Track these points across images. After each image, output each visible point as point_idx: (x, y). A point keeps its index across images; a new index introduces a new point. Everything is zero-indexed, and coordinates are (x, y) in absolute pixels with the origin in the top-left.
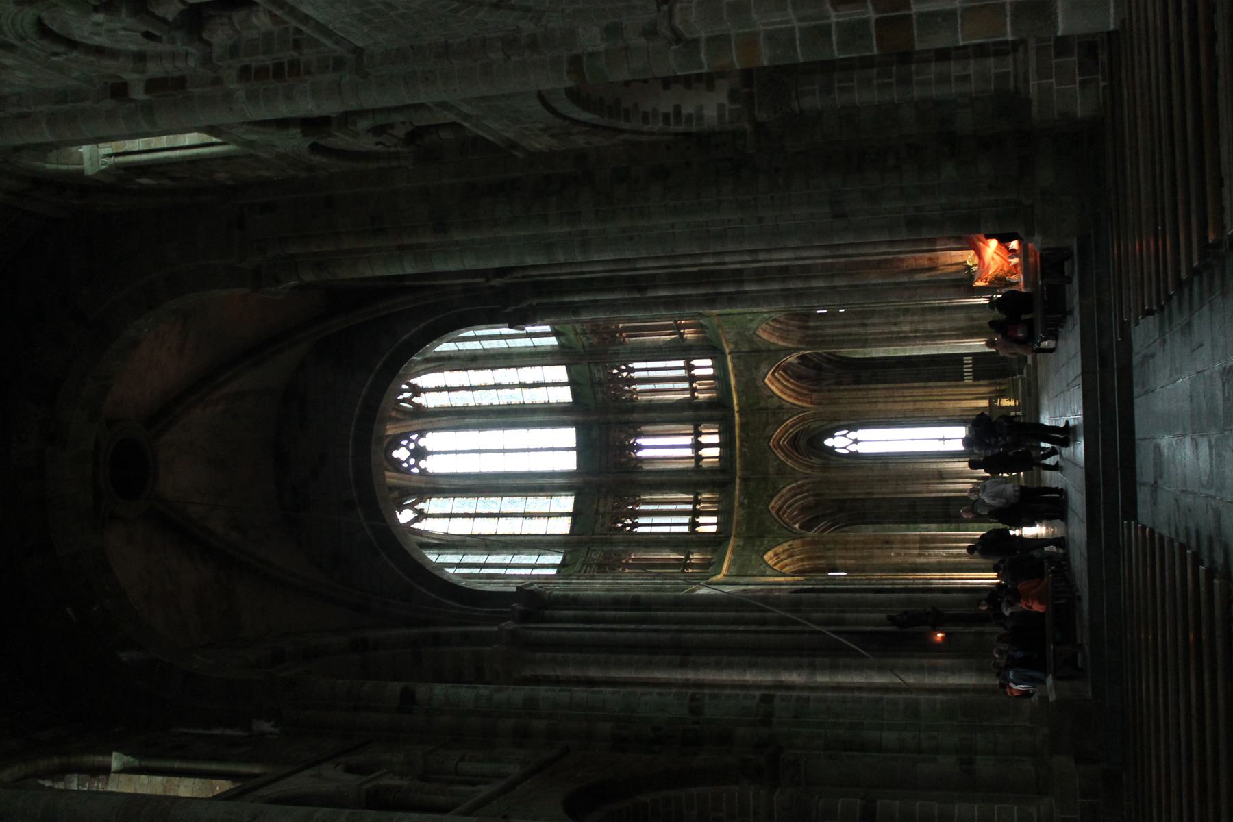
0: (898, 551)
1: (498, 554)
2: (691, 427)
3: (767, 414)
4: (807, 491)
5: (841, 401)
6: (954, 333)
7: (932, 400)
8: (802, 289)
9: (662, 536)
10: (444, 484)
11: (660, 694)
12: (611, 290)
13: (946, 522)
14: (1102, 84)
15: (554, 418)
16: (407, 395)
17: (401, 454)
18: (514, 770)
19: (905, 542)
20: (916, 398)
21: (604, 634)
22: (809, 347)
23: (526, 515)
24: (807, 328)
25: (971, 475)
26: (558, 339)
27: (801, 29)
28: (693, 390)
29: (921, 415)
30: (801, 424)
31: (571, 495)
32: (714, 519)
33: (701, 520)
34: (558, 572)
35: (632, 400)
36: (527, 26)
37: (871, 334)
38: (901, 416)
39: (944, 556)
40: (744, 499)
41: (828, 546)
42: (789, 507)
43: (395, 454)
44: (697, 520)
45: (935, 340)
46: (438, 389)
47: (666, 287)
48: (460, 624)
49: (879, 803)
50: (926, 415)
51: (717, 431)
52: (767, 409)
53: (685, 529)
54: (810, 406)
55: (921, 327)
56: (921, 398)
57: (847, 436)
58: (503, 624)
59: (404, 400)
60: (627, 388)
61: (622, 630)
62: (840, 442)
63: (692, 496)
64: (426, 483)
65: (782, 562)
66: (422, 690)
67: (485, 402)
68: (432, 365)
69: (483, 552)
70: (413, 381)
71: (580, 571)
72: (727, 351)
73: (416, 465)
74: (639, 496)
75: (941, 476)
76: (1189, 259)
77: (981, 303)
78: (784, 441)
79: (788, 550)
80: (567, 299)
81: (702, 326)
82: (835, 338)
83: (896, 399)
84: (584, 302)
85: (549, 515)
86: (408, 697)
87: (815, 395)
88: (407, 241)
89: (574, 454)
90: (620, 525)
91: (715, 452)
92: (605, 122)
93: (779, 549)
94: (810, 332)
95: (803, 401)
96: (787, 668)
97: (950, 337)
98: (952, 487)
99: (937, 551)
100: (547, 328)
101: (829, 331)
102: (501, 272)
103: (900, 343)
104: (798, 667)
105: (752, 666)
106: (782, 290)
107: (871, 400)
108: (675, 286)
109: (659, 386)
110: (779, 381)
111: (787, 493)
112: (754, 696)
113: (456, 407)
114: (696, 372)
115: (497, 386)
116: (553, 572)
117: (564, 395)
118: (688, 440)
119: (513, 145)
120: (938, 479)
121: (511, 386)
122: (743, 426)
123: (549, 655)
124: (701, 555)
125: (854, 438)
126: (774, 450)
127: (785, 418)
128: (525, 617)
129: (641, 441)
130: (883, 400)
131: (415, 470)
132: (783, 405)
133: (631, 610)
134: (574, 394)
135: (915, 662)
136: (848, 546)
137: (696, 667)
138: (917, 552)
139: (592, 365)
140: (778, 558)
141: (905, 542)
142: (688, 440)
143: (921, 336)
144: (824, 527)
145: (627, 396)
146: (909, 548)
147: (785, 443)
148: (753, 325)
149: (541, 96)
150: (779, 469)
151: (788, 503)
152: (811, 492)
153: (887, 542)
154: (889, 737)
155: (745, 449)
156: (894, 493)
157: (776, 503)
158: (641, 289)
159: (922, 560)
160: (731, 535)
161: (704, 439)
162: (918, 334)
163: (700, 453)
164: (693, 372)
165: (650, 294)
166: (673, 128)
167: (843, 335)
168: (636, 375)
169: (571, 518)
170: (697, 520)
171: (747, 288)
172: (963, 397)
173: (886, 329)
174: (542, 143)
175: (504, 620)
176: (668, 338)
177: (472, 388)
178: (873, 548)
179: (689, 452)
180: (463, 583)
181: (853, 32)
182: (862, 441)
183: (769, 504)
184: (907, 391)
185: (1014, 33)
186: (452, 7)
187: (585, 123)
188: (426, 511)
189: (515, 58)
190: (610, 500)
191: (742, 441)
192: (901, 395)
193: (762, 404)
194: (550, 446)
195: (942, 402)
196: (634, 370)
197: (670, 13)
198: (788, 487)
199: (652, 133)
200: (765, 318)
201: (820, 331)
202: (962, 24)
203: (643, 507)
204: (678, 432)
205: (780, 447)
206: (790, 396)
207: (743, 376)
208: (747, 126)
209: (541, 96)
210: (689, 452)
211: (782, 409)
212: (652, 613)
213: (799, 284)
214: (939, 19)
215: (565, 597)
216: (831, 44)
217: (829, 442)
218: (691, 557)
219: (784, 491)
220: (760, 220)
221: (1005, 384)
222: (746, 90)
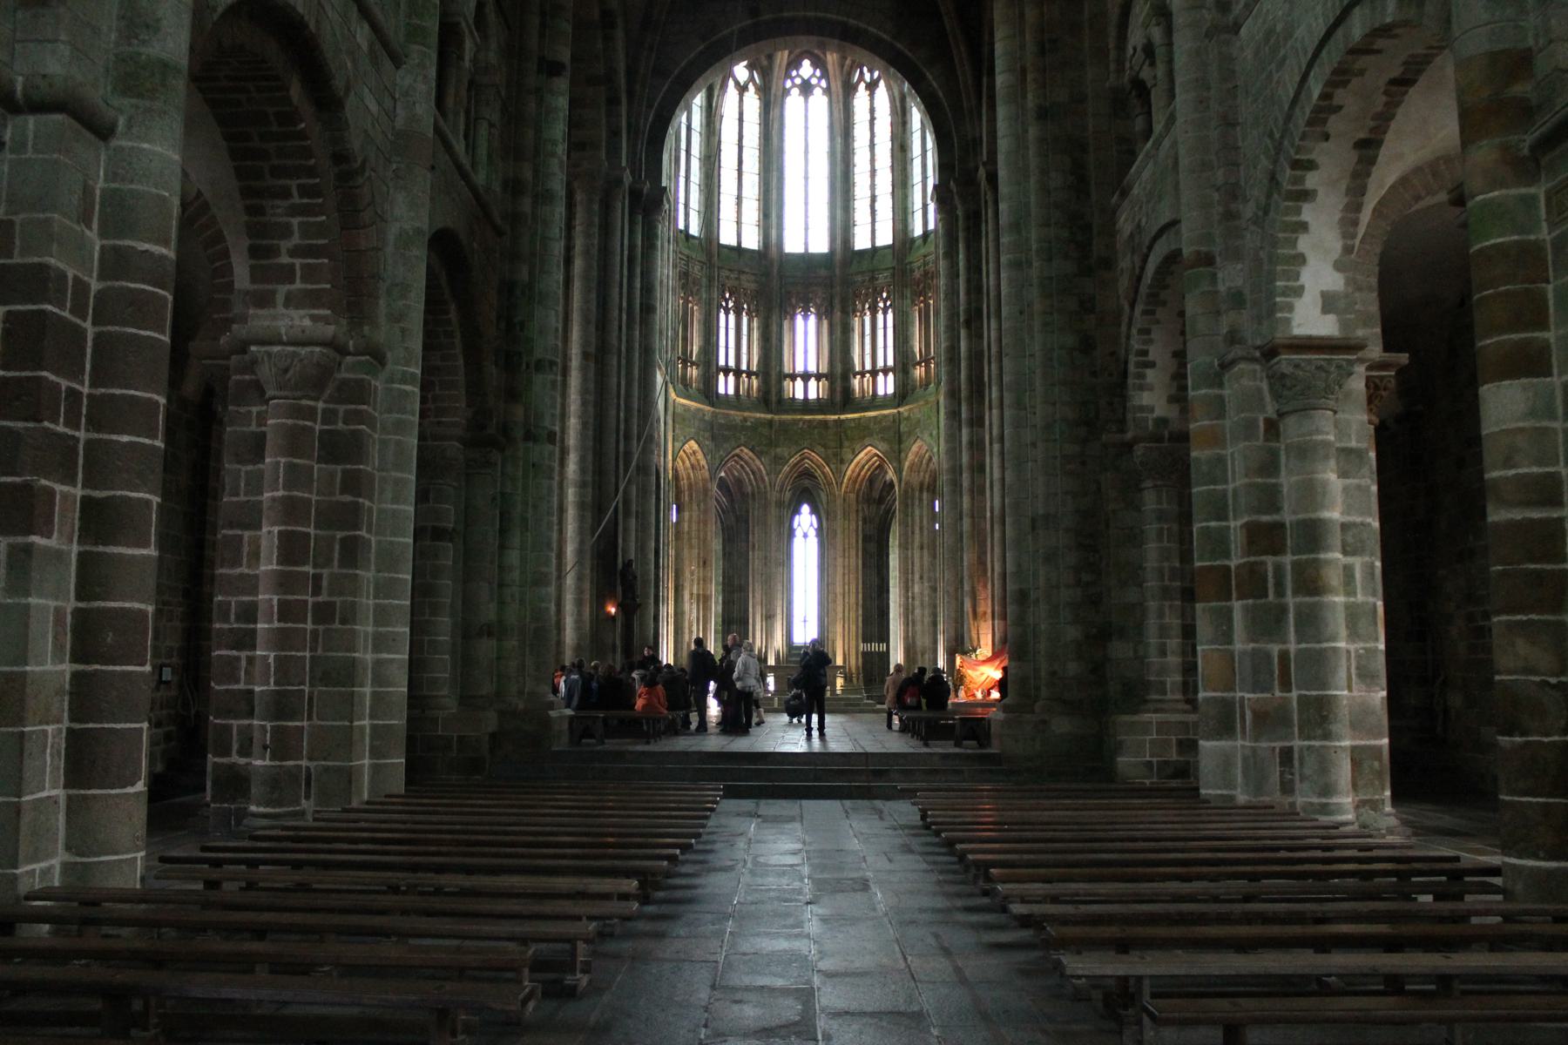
0: (696, 574)
1: (700, 168)
2: (825, 371)
4: (758, 487)
8: (961, 485)
10: (774, 113)
11: (557, 329)
12: (968, 293)
13: (723, 621)
14: (1147, 782)
15: (839, 232)
16: (867, 77)
17: (806, 69)
18: (480, 178)
19: (705, 580)
20: (847, 595)
21: (618, 277)
23: (739, 198)
24: (921, 491)
26: (919, 237)
27: (1225, 491)
28: (863, 374)
32: (731, 391)
33: (731, 378)
34: (681, 231)
35: (854, 311)
36: (1248, 210)
37: (913, 554)
42: (742, 466)
43: (806, 63)
44: (731, 374)
46: (872, 110)
47: (970, 350)
48: (629, 125)
49: (450, 545)
52: (841, 446)
53: (722, 362)
55: (917, 603)
56: (847, 600)
58: (628, 171)
59: (862, 73)
60: (867, 306)
61: (621, 294)
62: (805, 520)
64: (775, 95)
66: (562, 84)
68: (898, 104)
70: (882, 83)
71: (680, 253)
72: (901, 409)
73: (794, 85)
75: (769, 617)
76: (973, 851)
80: (961, 246)
81: (928, 384)
83: (847, 577)
84: (958, 264)
85: (739, 223)
86: (554, 69)
87: (853, 496)
88: (1029, 77)
89: (801, 250)
90: (727, 295)
91: (799, 395)
92: (1143, 290)
93: (700, 456)
94: (917, 494)
96: (582, 459)
98: (758, 627)
99: (695, 611)
100: (931, 226)
101: (917, 512)
102: (993, 178)
104: (582, 470)
105: (584, 425)
106: (961, 466)
108: (970, 358)
109: (868, 340)
112: (555, 425)
114: (881, 377)
115: (873, 172)
116: (681, 226)
117: (861, 242)
118: (812, 368)
119: (1124, 194)
121: (873, 186)
122: (825, 423)
123: (596, 220)
127: (833, 466)
128: (635, 194)
129: (812, 319)
130: (846, 564)
131: (789, 84)
133: (641, 304)
134: (862, 253)
135: (587, 585)
137: (584, 369)
138: (695, 592)
139: (891, 271)
141: (705, 580)
143: (908, 604)
145: (859, 307)
146: (698, 584)
148: (926, 436)
149: (1174, 223)
150: (780, 459)
153: (705, 563)
154: (513, 557)
155: (801, 423)
156: (753, 570)
158: (968, 323)
161: (812, 383)
163: (799, 379)
164: (881, 374)
165: (963, 333)
166: (1133, 359)
167: (913, 525)
168: (880, 316)
170: (731, 374)
171: (965, 432)
172: (846, 641)
173: (917, 568)
174: (1125, 225)
175: (632, 173)
176: (917, 350)
177: (872, 146)
178: (699, 548)
180: (671, 131)
181: (1219, 543)
185: (1207, 700)
186: (1275, 130)
187: (1142, 269)
188: (746, 94)
189: (1216, 196)
190: (753, 286)
191: (810, 421)
193: (846, 443)
194: (810, 226)
196: (885, 313)
197: (1253, 360)
199: (1128, 337)
202: (1218, 649)
203: (745, 320)
205: (803, 459)
206: (853, 471)
208: (1129, 435)
209: (1174, 223)
210: (800, 368)
212: (637, 327)
213: (966, 483)
214: (1225, 628)
215: (656, 236)
216: (1206, 520)
217: (805, 508)
220: (1034, 445)
222: (1166, 434)
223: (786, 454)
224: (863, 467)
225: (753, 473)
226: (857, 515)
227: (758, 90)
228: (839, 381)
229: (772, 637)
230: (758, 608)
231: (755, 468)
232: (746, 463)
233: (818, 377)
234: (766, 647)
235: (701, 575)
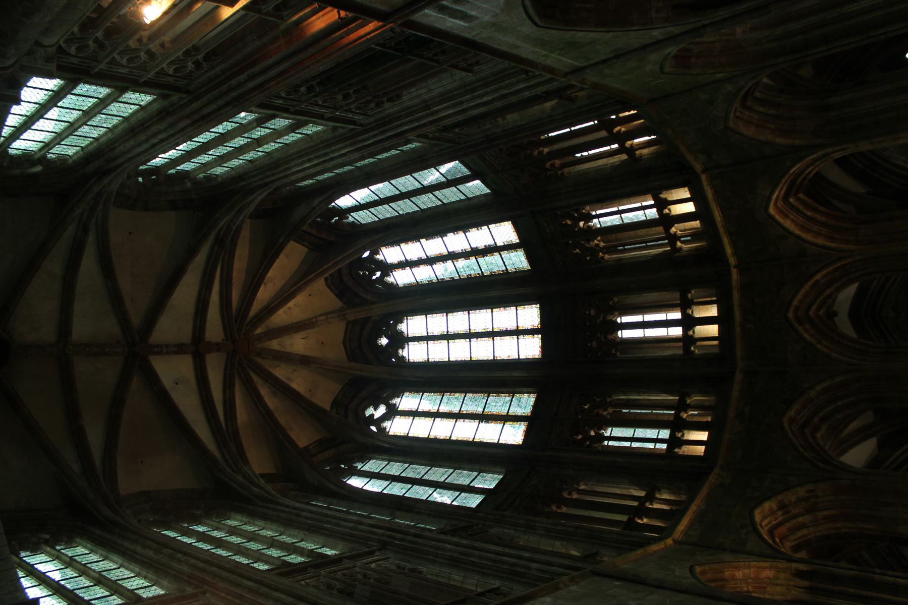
1: (440, 467)
9: (619, 459)
28: (673, 238)
31: (533, 393)
32: (703, 436)
51: (715, 299)
63: (677, 398)
65: (794, 521)
67: (447, 276)
69: (427, 462)
72: (698, 168)
74: (610, 396)
91: (713, 330)
93: (790, 497)
110: (798, 211)
113: (422, 284)
116: (473, 501)
117: (518, 261)
121: (466, 255)
124: (674, 493)
126: (796, 325)
142: (676, 315)
163: (691, 333)
164: (666, 211)
169: (526, 423)
179: (677, 331)
198: (819, 388)
204: (671, 303)
218: (658, 496)
224: (809, 219)
227: (399, 394)
233: (685, 305)
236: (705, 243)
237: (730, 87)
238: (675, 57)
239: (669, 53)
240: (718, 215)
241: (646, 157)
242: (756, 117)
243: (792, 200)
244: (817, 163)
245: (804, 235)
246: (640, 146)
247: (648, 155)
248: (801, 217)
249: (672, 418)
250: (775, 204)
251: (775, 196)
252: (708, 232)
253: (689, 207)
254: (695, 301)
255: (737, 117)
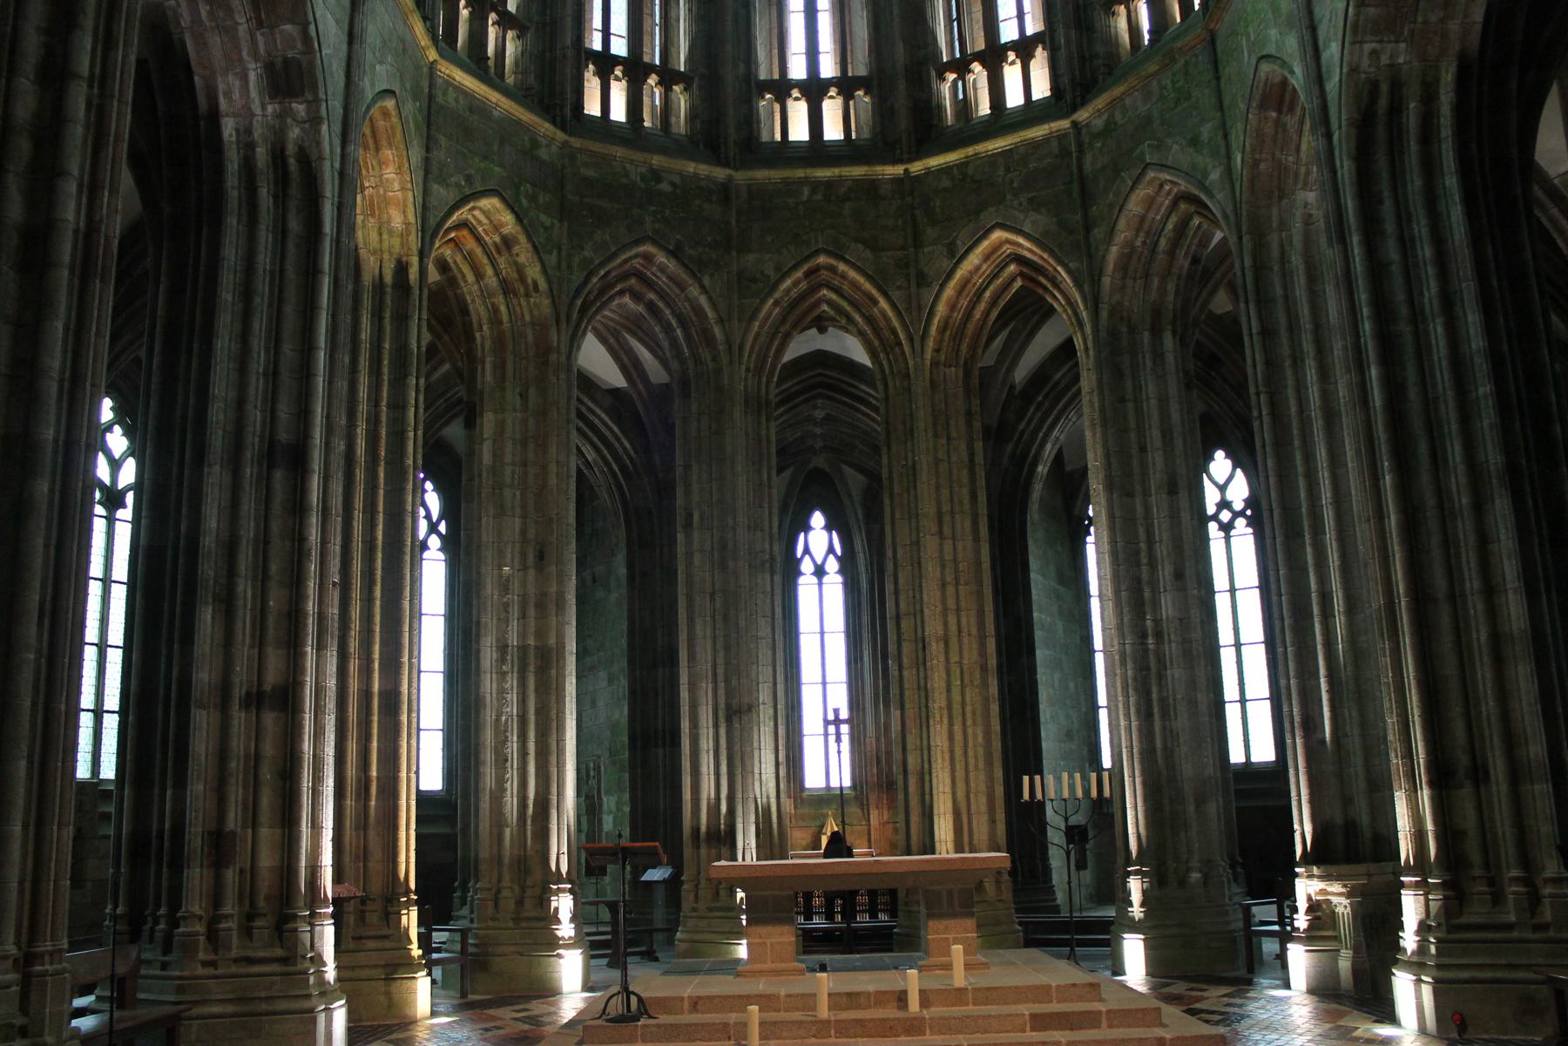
3: (902, 248)
4: (697, 360)
5: (943, 441)
6: (1159, 744)
7: (949, 690)
19: (543, 606)
22: (1103, 334)
24: (1156, 332)
25: (739, 795)
28: (961, 67)
29: (905, 661)
30: (876, 343)
32: (618, 113)
37: (1147, 509)
38: (902, 605)
39: (498, 720)
40: (673, 185)
41: (532, 391)
45: (1136, 690)
50: (906, 673)
52: (918, 244)
54: (928, 355)
55: (1172, 649)
56: (954, 658)
57: (831, 556)
62: (818, 538)
63: (682, 69)
65: (485, 261)
72: (1082, 115)
75: (736, 713)
77: (1296, 826)
78: (830, 303)
79: (522, 279)
82: (1130, 405)
83: (950, 590)
87: (954, 373)
91: (799, 131)
93: (523, 252)
95: (940, 342)
97: (1147, 735)
98: (706, 743)
99: (513, 697)
101: (1151, 389)
103: (1123, 587)
107: (947, 518)
111: (688, 299)
120: (728, 706)
122: (870, 188)
124: (516, 63)
125: (827, 568)
126: (806, 267)
127: (895, 295)
130: (948, 557)
132: (929, 285)
136: (531, 446)
138: (513, 640)
140: (499, 252)
141: (543, 606)
142: (828, 69)
143: (1146, 650)
144: (620, 450)
146: (523, 616)
147: (825, 307)
148: (1177, 152)
150: (754, 280)
151: (661, 304)
152: (691, 364)
153: (541, 556)
155: (806, 191)
156: (689, 584)
157: (662, 269)
159: (488, 655)
160: (570, 135)
161: (832, 110)
162: (1150, 640)
163: (795, 93)
164: (1011, 56)
172: (960, 774)
173: (1162, 550)
178: (524, 517)
179: (797, 70)
182: (820, 584)
183: (655, 243)
184: (973, 620)
191: (830, 184)
192: (963, 604)
195: (945, 712)
198: (703, 300)
200: (1206, 174)
201: (1149, 363)
206: (953, 307)
207: (1008, 170)
211: (919, 285)
217: (818, 519)
218: (510, 34)
219: (694, 291)
221: (999, 889)
223: (769, 270)
225: (683, 323)
226: (969, 425)
228: (902, 86)
229: (747, 771)
230: (706, 688)
231: (686, 308)
232: (662, 295)
233: (845, 86)
234: (731, 799)
235: (532, 590)
236: (949, 124)
237: (1215, 176)
238: (1284, 83)
239: (1292, 72)
240: (997, 146)
241: (1112, 24)
242: (1159, 217)
243: (1012, 267)
244: (1069, 311)
245: (952, 283)
246: (1133, 14)
247: (1116, 28)
248: (983, 282)
249: (646, 59)
250: (1008, 241)
251: (1021, 240)
252: (970, 130)
253: (1014, 98)
254: (851, 103)
255: (1161, 186)
